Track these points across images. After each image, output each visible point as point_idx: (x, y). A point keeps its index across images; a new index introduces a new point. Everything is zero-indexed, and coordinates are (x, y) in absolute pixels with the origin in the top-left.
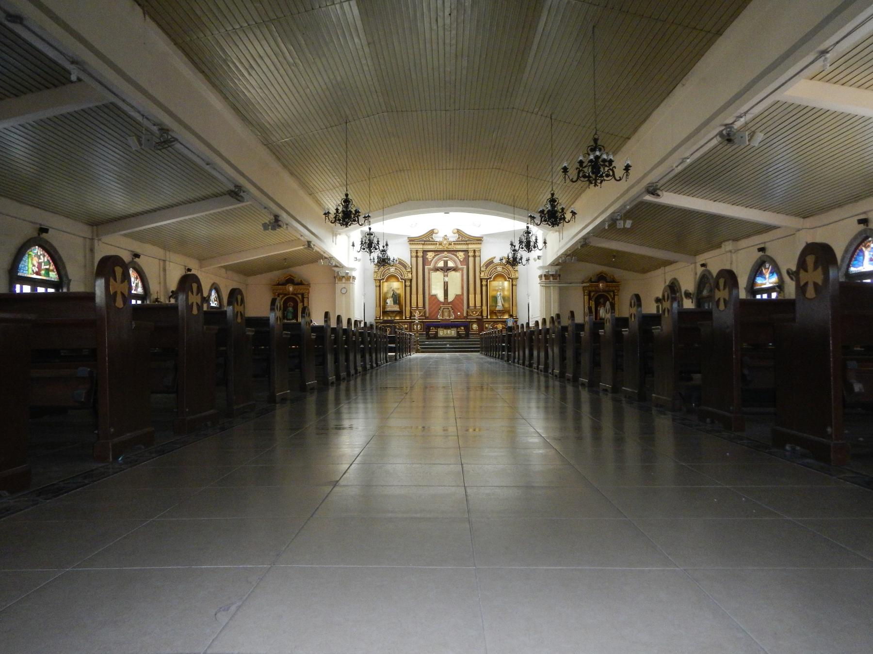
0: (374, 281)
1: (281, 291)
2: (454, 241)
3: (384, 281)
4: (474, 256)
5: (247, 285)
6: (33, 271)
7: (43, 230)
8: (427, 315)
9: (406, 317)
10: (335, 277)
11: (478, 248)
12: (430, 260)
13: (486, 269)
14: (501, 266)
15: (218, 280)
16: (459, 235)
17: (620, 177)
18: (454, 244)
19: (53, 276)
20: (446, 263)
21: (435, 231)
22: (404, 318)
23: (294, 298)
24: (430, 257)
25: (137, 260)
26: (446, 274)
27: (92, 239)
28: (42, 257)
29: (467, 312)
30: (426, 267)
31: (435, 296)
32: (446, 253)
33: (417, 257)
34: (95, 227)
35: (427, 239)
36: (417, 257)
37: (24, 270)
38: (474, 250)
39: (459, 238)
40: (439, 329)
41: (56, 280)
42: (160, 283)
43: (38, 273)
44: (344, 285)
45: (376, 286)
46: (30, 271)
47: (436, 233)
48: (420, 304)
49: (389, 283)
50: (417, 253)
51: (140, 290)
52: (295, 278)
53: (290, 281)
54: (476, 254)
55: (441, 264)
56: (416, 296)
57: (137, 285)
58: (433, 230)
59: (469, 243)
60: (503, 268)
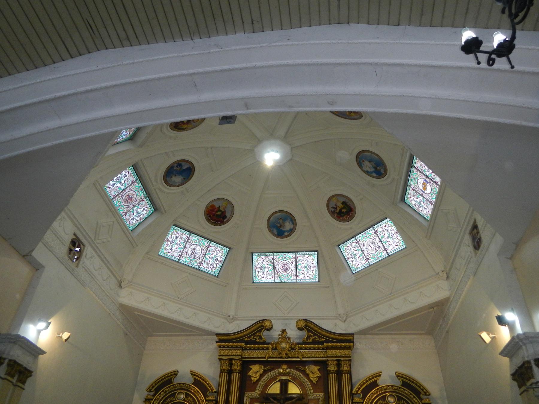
2: (299, 344)
4: (339, 373)
12: (254, 380)
13: (364, 398)
14: (394, 394)
16: (309, 331)
18: (301, 349)
21: (267, 324)
30: (247, 394)
32: (284, 367)
36: (230, 372)
38: (338, 361)
39: (308, 337)
47: (269, 329)
50: (231, 364)
54: (342, 368)
58: (263, 321)
59: (328, 347)
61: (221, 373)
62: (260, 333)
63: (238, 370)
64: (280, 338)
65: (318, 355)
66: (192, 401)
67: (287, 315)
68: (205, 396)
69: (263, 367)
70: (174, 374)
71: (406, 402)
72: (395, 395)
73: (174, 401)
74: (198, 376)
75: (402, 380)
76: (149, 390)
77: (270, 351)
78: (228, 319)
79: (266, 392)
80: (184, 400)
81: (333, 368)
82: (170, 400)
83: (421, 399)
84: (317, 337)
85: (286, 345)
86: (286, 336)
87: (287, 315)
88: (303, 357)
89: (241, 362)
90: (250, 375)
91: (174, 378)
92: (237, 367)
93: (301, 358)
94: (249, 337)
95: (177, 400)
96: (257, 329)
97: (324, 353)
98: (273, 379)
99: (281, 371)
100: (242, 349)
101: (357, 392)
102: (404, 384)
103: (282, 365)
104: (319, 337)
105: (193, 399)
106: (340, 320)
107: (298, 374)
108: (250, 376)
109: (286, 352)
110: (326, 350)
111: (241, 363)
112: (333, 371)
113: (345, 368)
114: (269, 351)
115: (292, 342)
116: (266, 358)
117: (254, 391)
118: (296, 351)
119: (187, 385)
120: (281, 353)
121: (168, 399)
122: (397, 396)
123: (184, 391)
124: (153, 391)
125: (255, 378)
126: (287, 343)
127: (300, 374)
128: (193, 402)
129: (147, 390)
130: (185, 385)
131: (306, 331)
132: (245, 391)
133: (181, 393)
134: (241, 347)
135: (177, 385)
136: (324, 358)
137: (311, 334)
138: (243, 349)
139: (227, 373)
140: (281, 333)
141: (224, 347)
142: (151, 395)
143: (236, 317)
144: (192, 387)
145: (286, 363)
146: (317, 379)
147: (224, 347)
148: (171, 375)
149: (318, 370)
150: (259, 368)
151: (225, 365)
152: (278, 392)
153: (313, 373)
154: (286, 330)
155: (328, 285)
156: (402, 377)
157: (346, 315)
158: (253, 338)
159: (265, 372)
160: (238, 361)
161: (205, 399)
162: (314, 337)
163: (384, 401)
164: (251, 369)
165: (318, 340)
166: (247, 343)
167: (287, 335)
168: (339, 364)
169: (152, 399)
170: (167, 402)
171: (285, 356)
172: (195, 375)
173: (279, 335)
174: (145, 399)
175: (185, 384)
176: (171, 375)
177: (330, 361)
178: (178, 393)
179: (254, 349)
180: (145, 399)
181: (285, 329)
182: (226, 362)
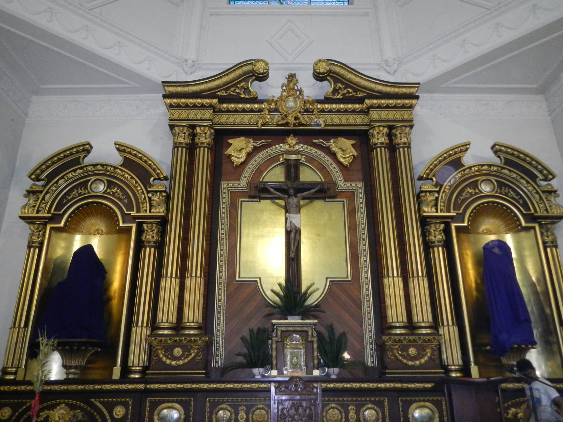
0: (22, 222)
2: (319, 102)
3: (62, 224)
4: (392, 148)
9: (126, 370)
11: (403, 121)
14: (493, 179)
16: (336, 80)
22: (117, 373)
29: (381, 348)
30: (224, 184)
32: (292, 140)
33: (192, 148)
35: (231, 92)
36: (192, 148)
38: (391, 128)
39: (335, 91)
45: (29, 247)
47: (262, 77)
50: (193, 136)
54: (398, 141)
56: (176, 283)
59: (372, 107)
60: (501, 185)
61: (176, 149)
62: (246, 83)
63: (208, 144)
64: (285, 90)
65: (351, 121)
66: (121, 194)
67: (293, 61)
68: (146, 184)
69: (252, 141)
70: (84, 150)
71: (511, 191)
72: (493, 180)
73: (85, 194)
74: (130, 153)
75: (504, 157)
76: (33, 176)
77: (266, 114)
78: (185, 66)
79: (261, 180)
80: (105, 192)
81: (382, 140)
82: (77, 192)
83: (539, 186)
84: (351, 91)
85: (295, 102)
86: (295, 86)
87: (293, 61)
88: (326, 125)
89: (212, 131)
90: (230, 153)
91: (85, 156)
92: (206, 139)
93: (323, 125)
94: (226, 90)
95: (90, 192)
96: (240, 76)
97: (363, 117)
98: (272, 160)
99: (287, 147)
100: (214, 112)
101: (428, 174)
102: (508, 162)
103: (288, 138)
104: (356, 91)
105: (122, 189)
106: (386, 71)
107: (316, 152)
108: (230, 155)
109: (296, 114)
110: (368, 112)
111: (211, 134)
112: (381, 143)
113: (404, 140)
114: (263, 113)
115: (306, 98)
116: (259, 124)
117: (239, 180)
118: (314, 113)
119: (109, 168)
120: (286, 116)
121: (74, 191)
122: (496, 181)
123: (104, 178)
124: (43, 180)
125: (238, 158)
126: (297, 99)
127: (319, 152)
128: (123, 195)
129: (30, 177)
130: (105, 167)
131: (332, 82)
132: (221, 181)
133: (98, 181)
134: (211, 106)
135: (89, 168)
136: (363, 125)
137: (340, 85)
138: (217, 111)
139: (187, 149)
140: (286, 81)
141: (179, 106)
142: (38, 186)
143: (198, 64)
144: (121, 170)
145: (296, 133)
146: (350, 159)
147: (179, 106)
148: (78, 152)
149: (353, 145)
150: (246, 143)
151: (183, 135)
152: (282, 179)
153: (343, 151)
154: (296, 75)
155: (367, 11)
156: (507, 153)
157: (399, 60)
158: (234, 91)
159: (256, 150)
160: (207, 128)
161: (146, 189)
162: (345, 91)
163: (475, 190)
164: (231, 144)
165: (353, 95)
166: (222, 100)
167: (297, 84)
168: (390, 136)
169: (41, 192)
170: (71, 196)
171: (294, 122)
172: (124, 151)
173: (283, 85)
174: (27, 191)
175: (106, 165)
176: (78, 152)
177: (376, 128)
178: (92, 180)
179: (236, 111)
180: (27, 191)
181: (295, 74)
182: (183, 130)
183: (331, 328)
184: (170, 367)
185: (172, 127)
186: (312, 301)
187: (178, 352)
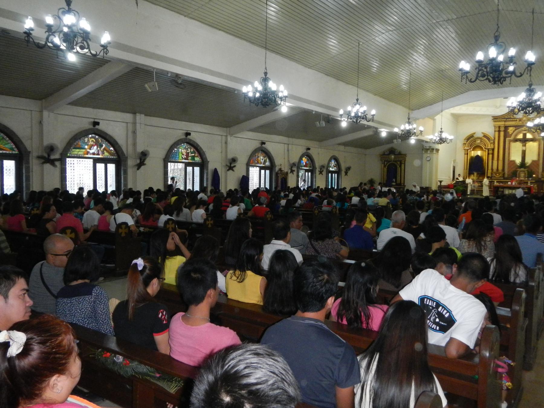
0: (463, 150)
1: (386, 159)
5: (365, 155)
6: (182, 158)
7: (188, 134)
8: (506, 176)
10: (423, 150)
12: (510, 133)
15: (336, 154)
17: (520, 73)
19: (198, 159)
20: (525, 135)
23: (394, 164)
24: (510, 131)
25: (264, 145)
26: (524, 144)
27: (226, 136)
28: (189, 149)
30: (507, 139)
31: (514, 162)
33: (499, 131)
34: (228, 129)
35: (509, 117)
36: (499, 131)
37: (175, 158)
40: (505, 190)
41: (200, 162)
42: (284, 158)
43: (185, 159)
44: (428, 155)
45: (465, 154)
46: (180, 158)
48: (500, 168)
49: (475, 152)
51: (268, 164)
52: (395, 150)
53: (392, 151)
55: (520, 136)
57: (265, 162)
68: (489, 141)
98: (520, 132)
123: (479, 140)
132: (507, 138)
138: (505, 121)
147: (496, 121)
183: (531, 170)
184: (496, 177)
185: (495, 127)
186: (528, 165)
187: (498, 174)
